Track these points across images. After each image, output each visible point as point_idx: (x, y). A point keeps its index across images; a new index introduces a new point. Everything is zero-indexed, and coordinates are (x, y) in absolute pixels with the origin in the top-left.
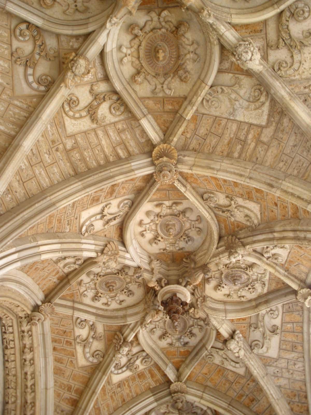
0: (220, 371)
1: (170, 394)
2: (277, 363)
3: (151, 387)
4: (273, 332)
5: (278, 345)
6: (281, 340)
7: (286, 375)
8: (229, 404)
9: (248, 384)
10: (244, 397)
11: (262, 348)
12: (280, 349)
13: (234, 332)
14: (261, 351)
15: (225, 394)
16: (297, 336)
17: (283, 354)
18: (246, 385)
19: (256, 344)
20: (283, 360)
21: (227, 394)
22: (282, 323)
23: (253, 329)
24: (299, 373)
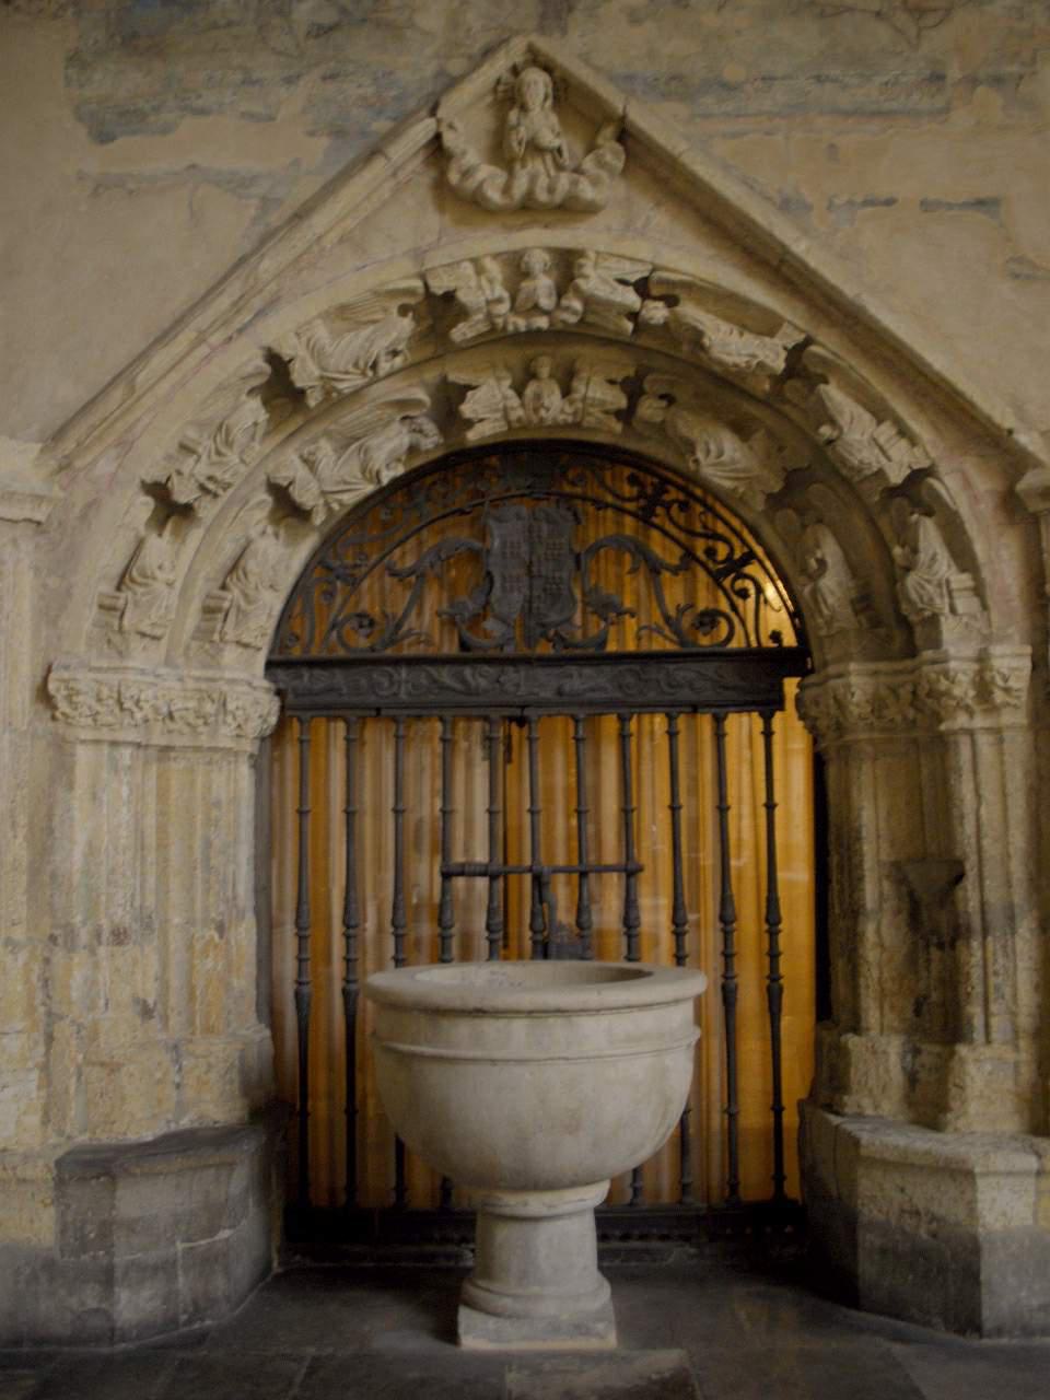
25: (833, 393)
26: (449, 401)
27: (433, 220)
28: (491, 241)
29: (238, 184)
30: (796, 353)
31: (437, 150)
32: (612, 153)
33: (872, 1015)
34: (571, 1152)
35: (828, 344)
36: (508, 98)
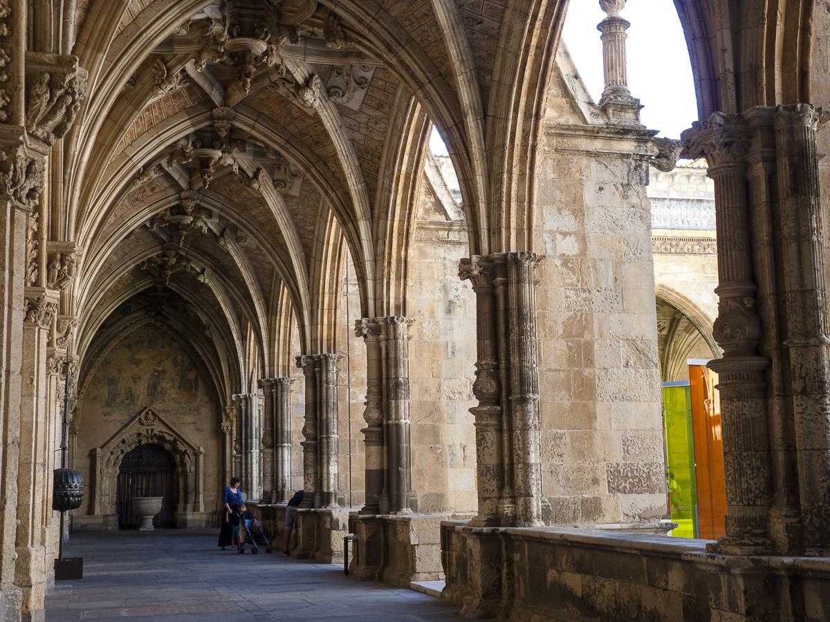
0: (282, 102)
1: (211, 118)
2: (356, 116)
3: (187, 107)
4: (359, 84)
5: (362, 98)
6: (366, 94)
7: (364, 131)
8: (287, 142)
9: (316, 126)
10: (308, 137)
11: (342, 96)
12: (363, 103)
13: (311, 76)
14: (339, 100)
15: (284, 127)
16: (387, 96)
17: (365, 109)
18: (313, 126)
19: (336, 92)
20: (364, 115)
21: (286, 127)
22: (373, 77)
23: (335, 74)
24: (380, 133)
25: (178, 442)
26: (140, 441)
27: (139, 425)
28: (145, 428)
29: (119, 421)
30: (174, 439)
31: (140, 419)
32: (157, 419)
33: (181, 502)
34: (151, 512)
35: (177, 438)
36: (147, 413)
